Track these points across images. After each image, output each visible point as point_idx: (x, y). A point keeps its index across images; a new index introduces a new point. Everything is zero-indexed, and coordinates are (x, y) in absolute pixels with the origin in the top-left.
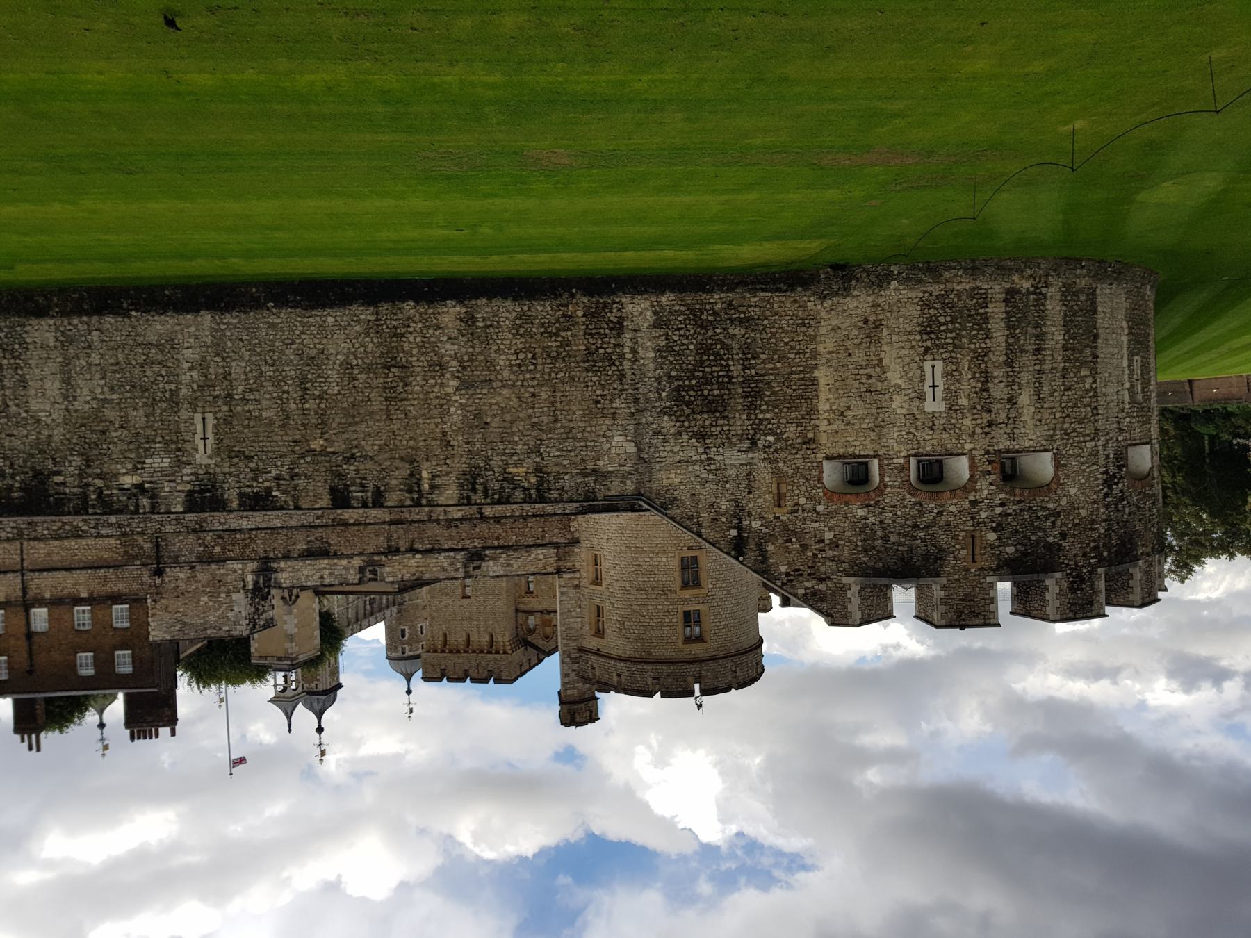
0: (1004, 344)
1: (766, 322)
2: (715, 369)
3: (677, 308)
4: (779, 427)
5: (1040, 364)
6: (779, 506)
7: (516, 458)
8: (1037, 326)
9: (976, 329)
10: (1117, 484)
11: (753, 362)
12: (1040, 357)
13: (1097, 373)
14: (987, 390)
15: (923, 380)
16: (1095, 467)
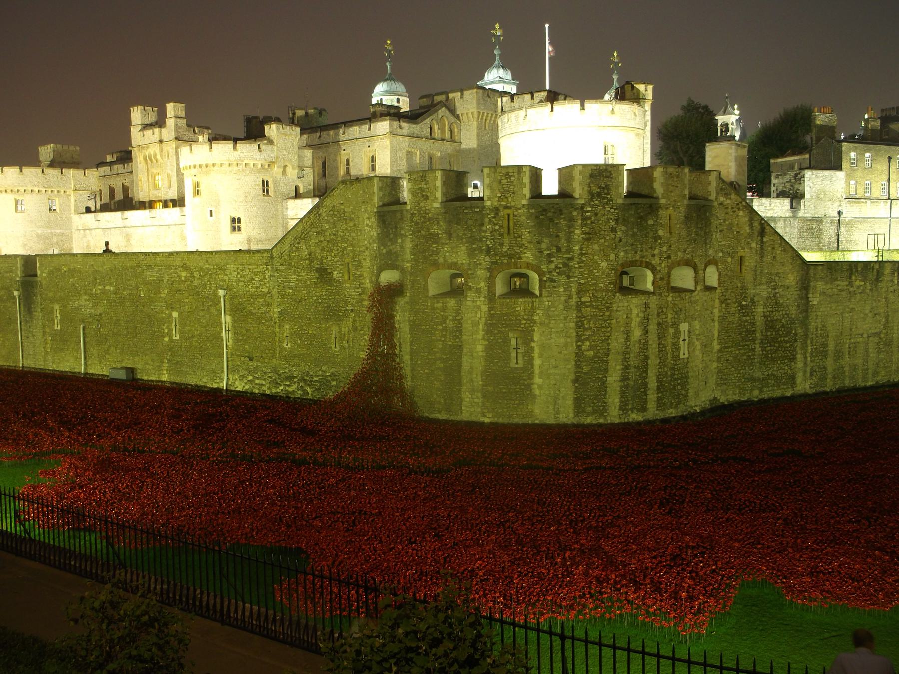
0: (649, 372)
1: (743, 380)
2: (769, 349)
3: (785, 387)
4: (739, 310)
5: (626, 358)
6: (741, 257)
7: (860, 291)
8: (627, 387)
9: (664, 382)
10: (557, 267)
11: (750, 354)
12: (626, 364)
13: (577, 354)
14: (659, 339)
15: (689, 344)
16: (582, 281)
